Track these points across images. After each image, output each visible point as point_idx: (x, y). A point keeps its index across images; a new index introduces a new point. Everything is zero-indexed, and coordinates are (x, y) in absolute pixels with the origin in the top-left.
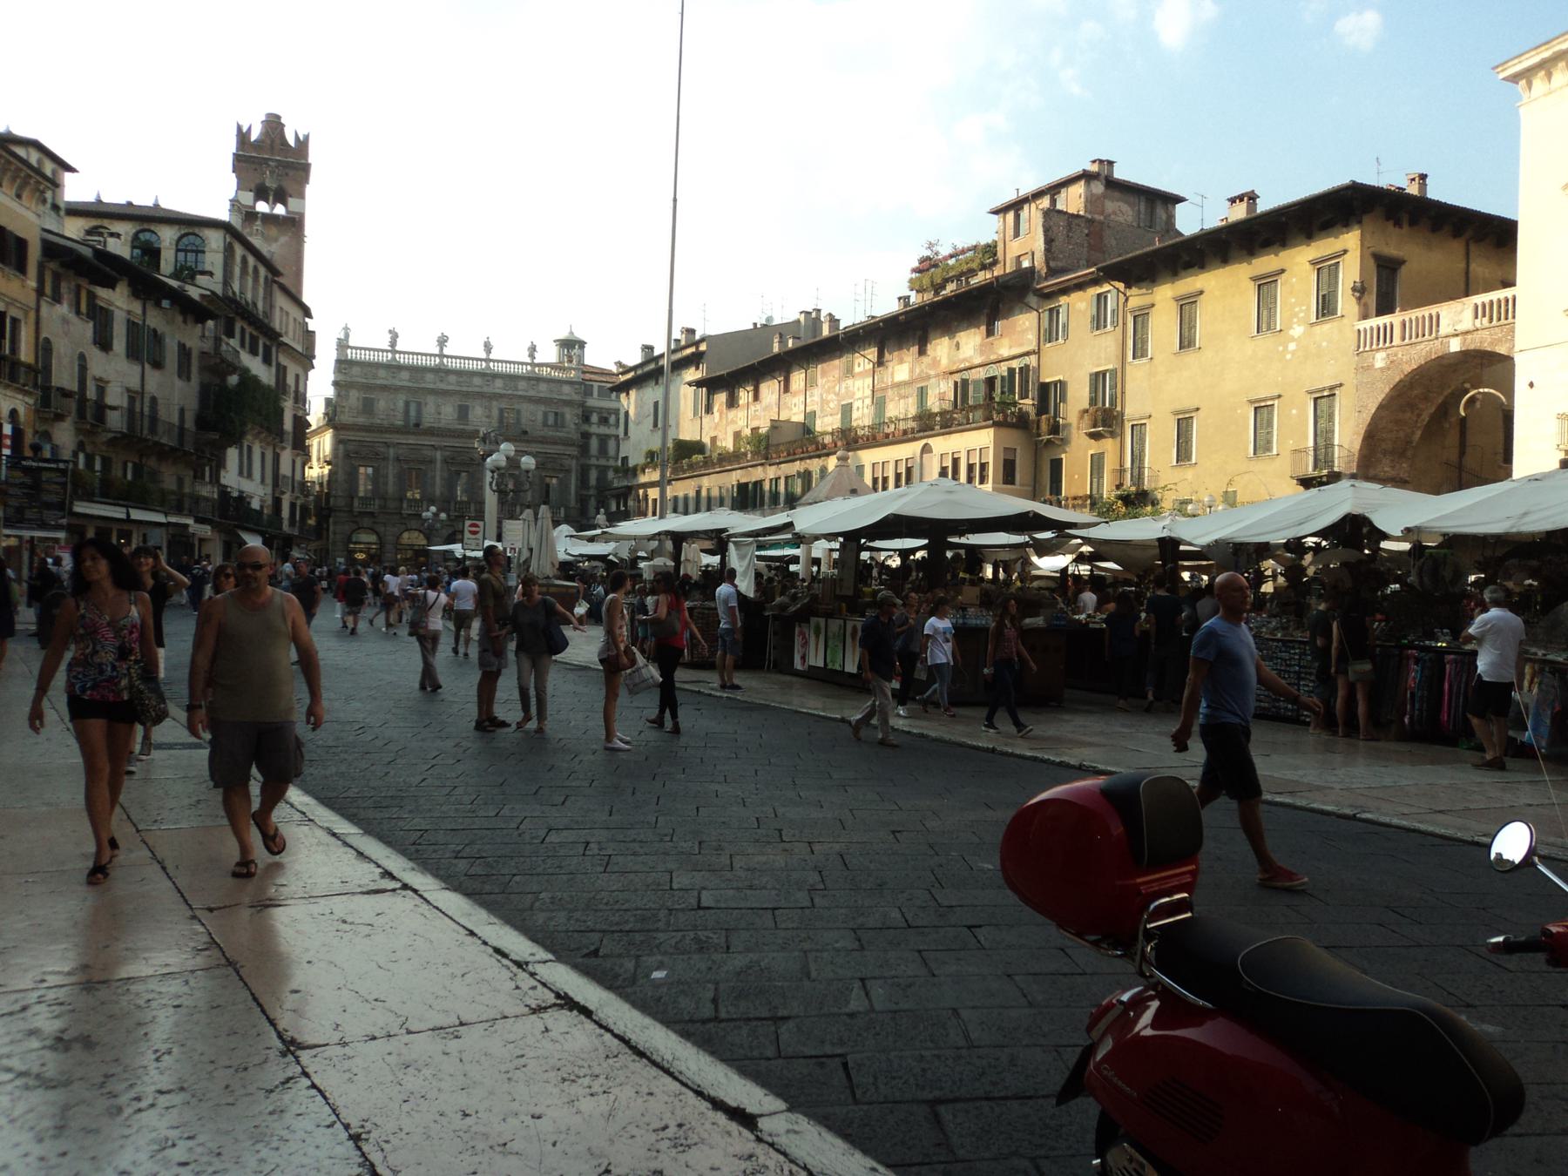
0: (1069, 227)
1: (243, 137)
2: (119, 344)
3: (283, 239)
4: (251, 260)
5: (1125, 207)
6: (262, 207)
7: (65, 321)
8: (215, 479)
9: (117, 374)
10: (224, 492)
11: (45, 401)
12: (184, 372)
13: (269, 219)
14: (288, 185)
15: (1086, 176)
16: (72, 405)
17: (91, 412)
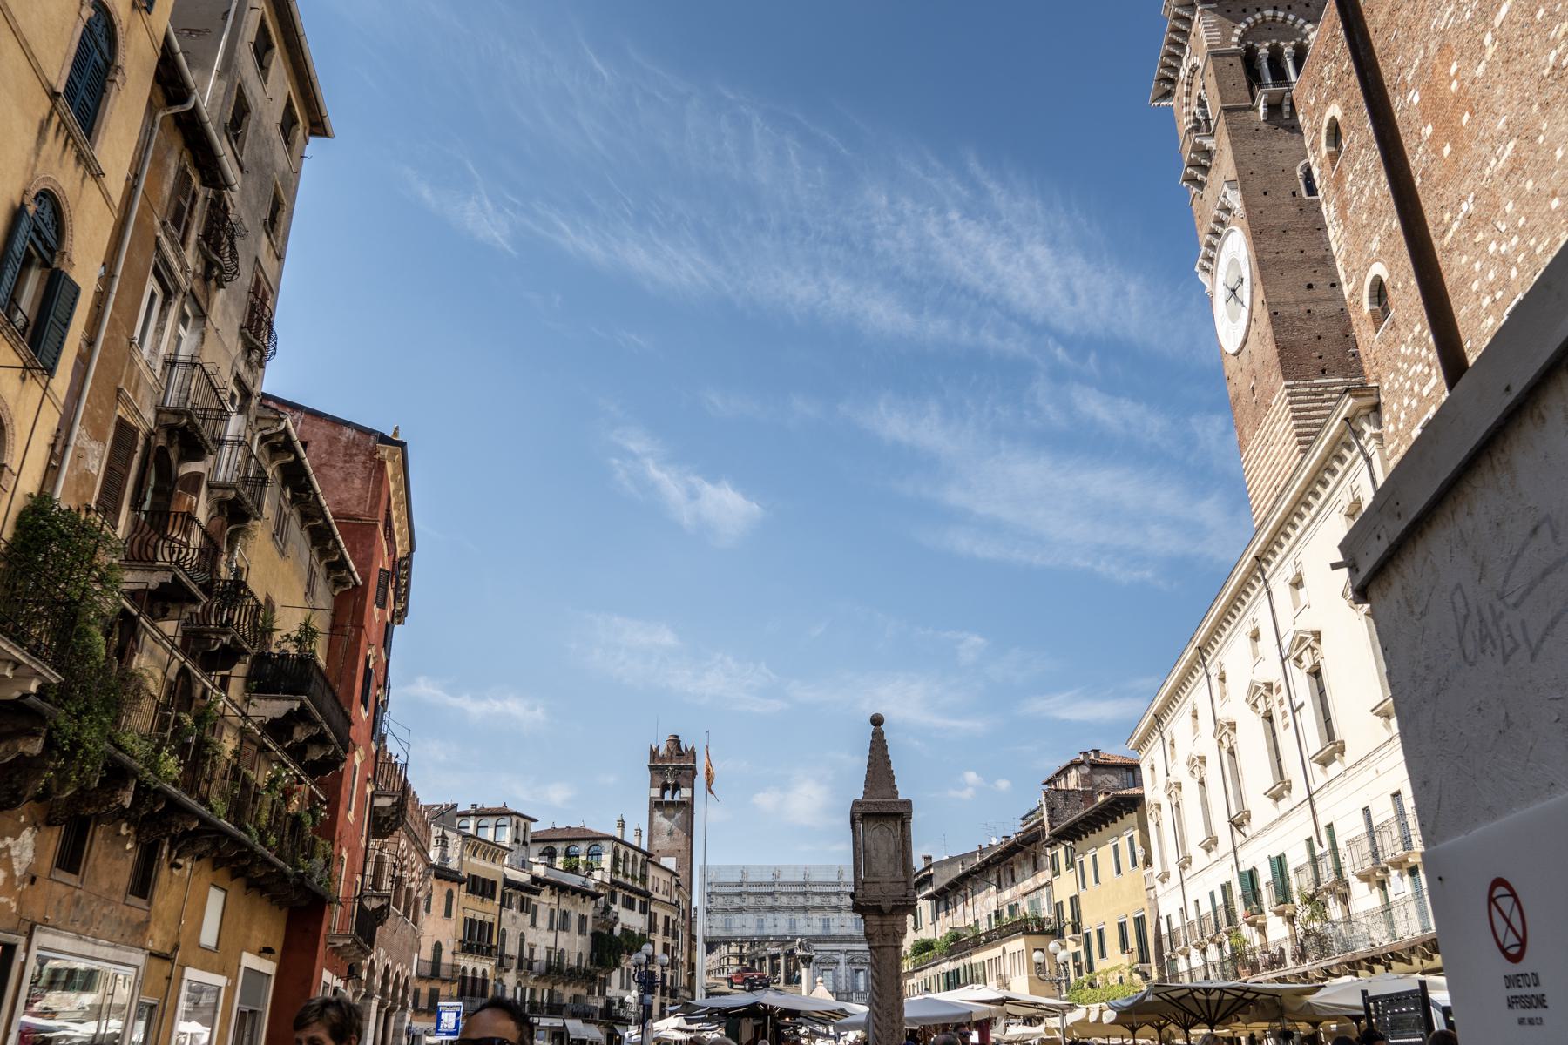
0: (1066, 798)
1: (654, 754)
2: (543, 922)
3: (678, 816)
4: (631, 852)
5: (1111, 777)
6: (668, 796)
7: (514, 917)
8: (602, 993)
9: (541, 940)
10: (610, 1003)
11: (501, 964)
12: (582, 931)
13: (671, 804)
14: (682, 781)
15: (1075, 764)
16: (515, 962)
17: (525, 965)
